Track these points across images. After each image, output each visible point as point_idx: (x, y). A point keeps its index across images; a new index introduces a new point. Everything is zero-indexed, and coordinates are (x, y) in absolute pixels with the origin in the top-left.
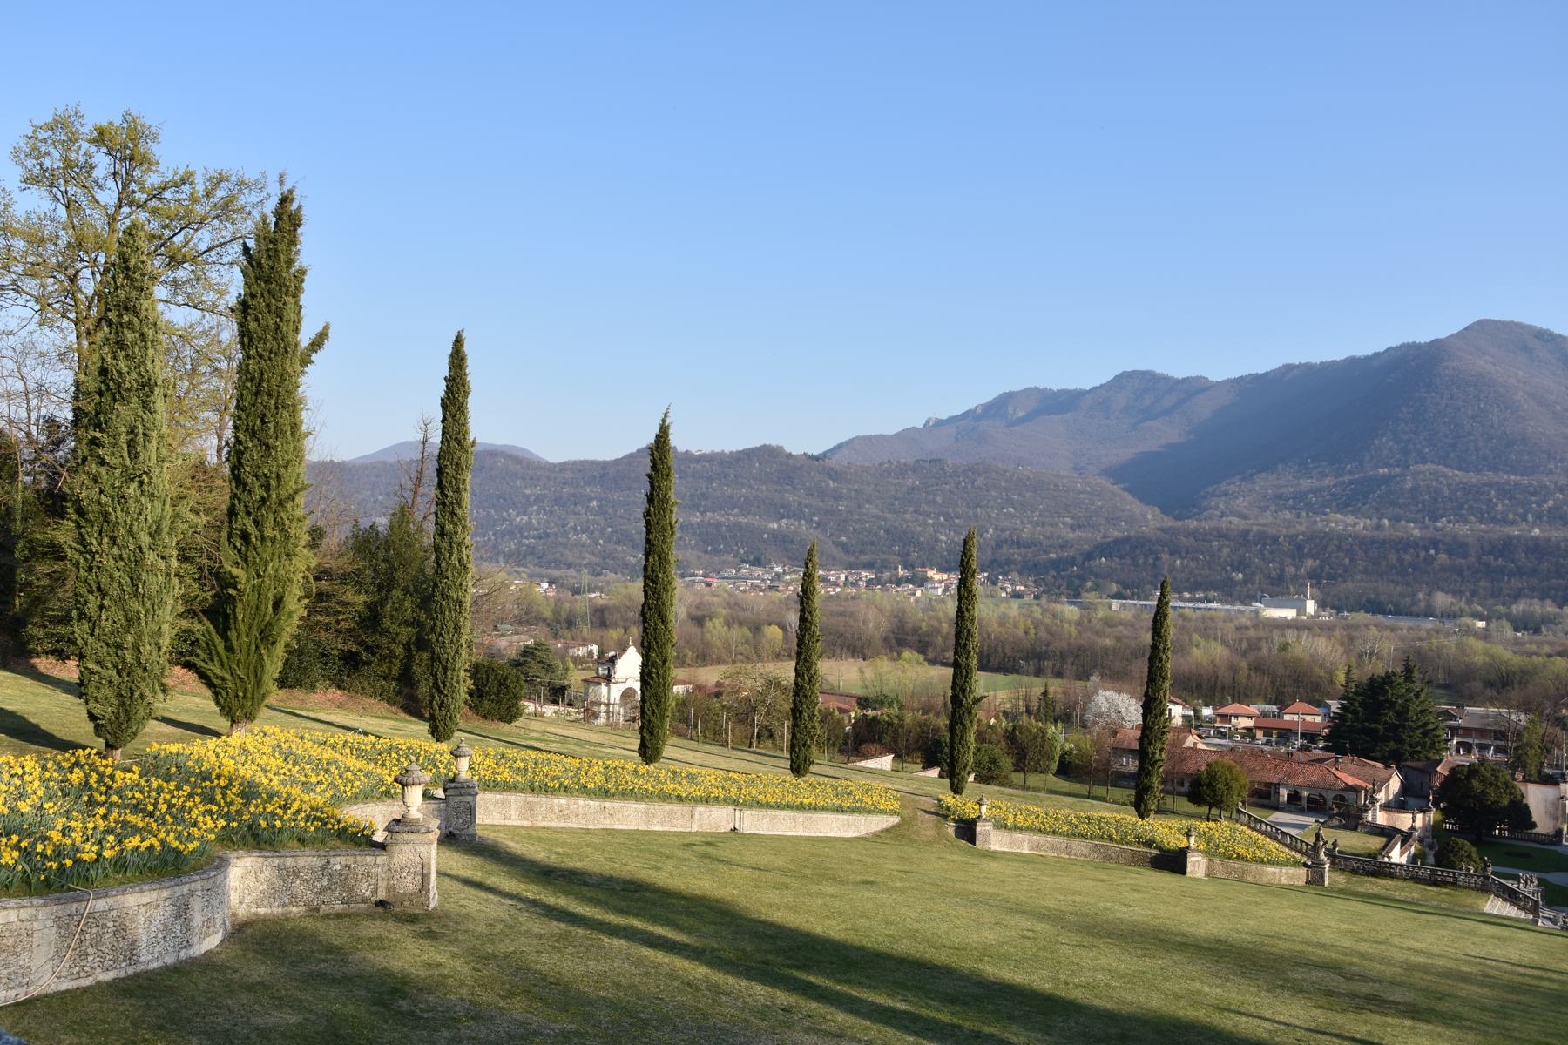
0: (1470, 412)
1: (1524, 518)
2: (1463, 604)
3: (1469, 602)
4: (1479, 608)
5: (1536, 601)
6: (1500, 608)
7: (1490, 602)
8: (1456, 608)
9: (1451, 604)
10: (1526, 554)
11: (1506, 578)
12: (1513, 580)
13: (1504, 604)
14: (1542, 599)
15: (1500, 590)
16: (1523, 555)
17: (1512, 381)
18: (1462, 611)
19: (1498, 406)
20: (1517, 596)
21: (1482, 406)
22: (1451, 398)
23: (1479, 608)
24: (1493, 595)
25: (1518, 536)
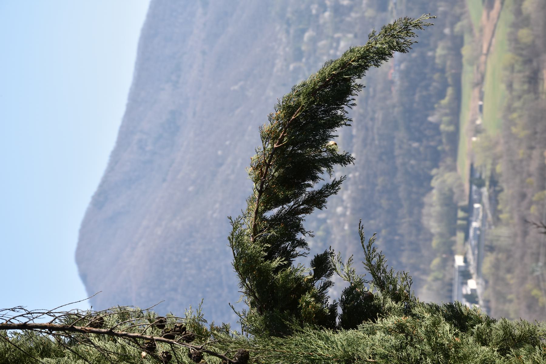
0: (193, 272)
1: (324, 221)
2: (429, 279)
3: (426, 272)
4: (436, 261)
5: (425, 211)
6: (435, 243)
7: (425, 253)
8: (436, 285)
9: (429, 289)
10: (371, 219)
11: (397, 238)
12: (400, 231)
13: (430, 240)
14: (421, 205)
15: (411, 243)
16: (372, 222)
17: (159, 231)
18: (436, 279)
19: (188, 244)
20: (418, 227)
21: (186, 260)
22: (175, 290)
23: (436, 261)
24: (416, 250)
25: (351, 226)
